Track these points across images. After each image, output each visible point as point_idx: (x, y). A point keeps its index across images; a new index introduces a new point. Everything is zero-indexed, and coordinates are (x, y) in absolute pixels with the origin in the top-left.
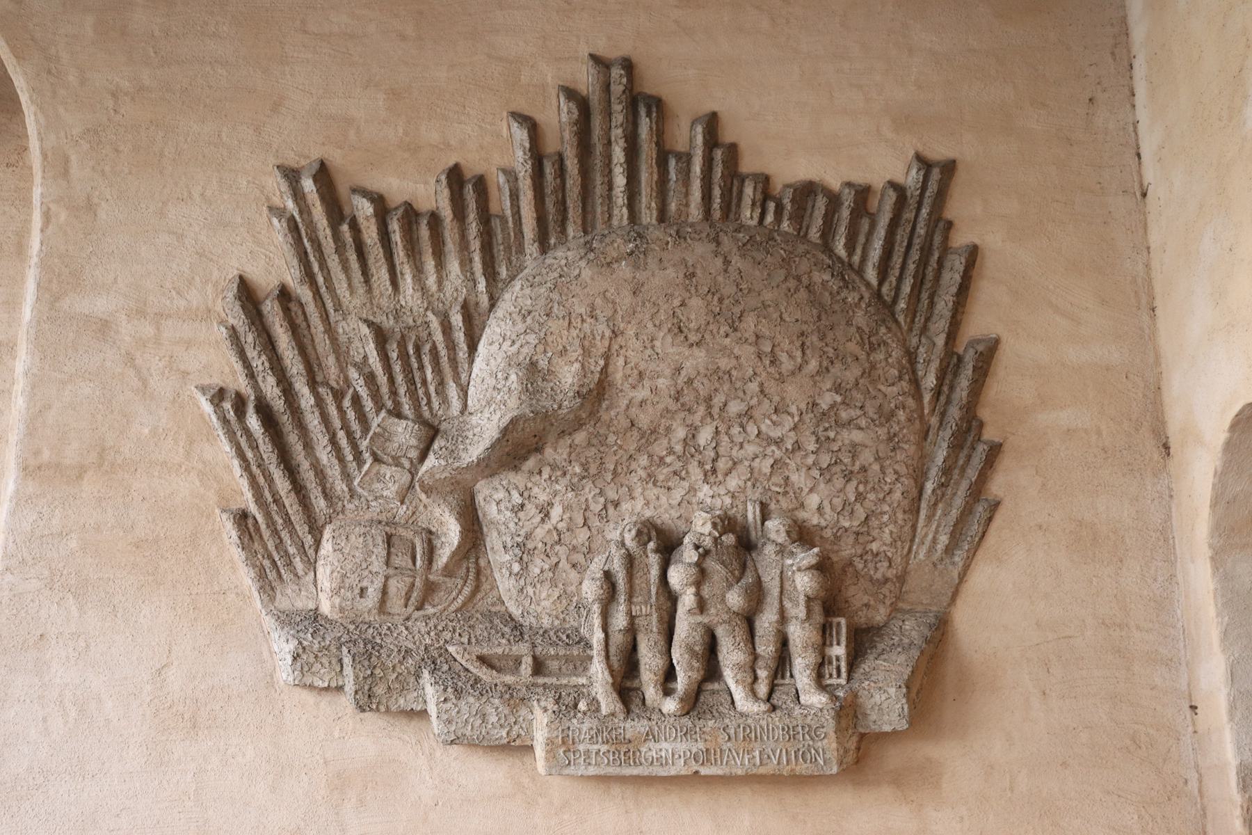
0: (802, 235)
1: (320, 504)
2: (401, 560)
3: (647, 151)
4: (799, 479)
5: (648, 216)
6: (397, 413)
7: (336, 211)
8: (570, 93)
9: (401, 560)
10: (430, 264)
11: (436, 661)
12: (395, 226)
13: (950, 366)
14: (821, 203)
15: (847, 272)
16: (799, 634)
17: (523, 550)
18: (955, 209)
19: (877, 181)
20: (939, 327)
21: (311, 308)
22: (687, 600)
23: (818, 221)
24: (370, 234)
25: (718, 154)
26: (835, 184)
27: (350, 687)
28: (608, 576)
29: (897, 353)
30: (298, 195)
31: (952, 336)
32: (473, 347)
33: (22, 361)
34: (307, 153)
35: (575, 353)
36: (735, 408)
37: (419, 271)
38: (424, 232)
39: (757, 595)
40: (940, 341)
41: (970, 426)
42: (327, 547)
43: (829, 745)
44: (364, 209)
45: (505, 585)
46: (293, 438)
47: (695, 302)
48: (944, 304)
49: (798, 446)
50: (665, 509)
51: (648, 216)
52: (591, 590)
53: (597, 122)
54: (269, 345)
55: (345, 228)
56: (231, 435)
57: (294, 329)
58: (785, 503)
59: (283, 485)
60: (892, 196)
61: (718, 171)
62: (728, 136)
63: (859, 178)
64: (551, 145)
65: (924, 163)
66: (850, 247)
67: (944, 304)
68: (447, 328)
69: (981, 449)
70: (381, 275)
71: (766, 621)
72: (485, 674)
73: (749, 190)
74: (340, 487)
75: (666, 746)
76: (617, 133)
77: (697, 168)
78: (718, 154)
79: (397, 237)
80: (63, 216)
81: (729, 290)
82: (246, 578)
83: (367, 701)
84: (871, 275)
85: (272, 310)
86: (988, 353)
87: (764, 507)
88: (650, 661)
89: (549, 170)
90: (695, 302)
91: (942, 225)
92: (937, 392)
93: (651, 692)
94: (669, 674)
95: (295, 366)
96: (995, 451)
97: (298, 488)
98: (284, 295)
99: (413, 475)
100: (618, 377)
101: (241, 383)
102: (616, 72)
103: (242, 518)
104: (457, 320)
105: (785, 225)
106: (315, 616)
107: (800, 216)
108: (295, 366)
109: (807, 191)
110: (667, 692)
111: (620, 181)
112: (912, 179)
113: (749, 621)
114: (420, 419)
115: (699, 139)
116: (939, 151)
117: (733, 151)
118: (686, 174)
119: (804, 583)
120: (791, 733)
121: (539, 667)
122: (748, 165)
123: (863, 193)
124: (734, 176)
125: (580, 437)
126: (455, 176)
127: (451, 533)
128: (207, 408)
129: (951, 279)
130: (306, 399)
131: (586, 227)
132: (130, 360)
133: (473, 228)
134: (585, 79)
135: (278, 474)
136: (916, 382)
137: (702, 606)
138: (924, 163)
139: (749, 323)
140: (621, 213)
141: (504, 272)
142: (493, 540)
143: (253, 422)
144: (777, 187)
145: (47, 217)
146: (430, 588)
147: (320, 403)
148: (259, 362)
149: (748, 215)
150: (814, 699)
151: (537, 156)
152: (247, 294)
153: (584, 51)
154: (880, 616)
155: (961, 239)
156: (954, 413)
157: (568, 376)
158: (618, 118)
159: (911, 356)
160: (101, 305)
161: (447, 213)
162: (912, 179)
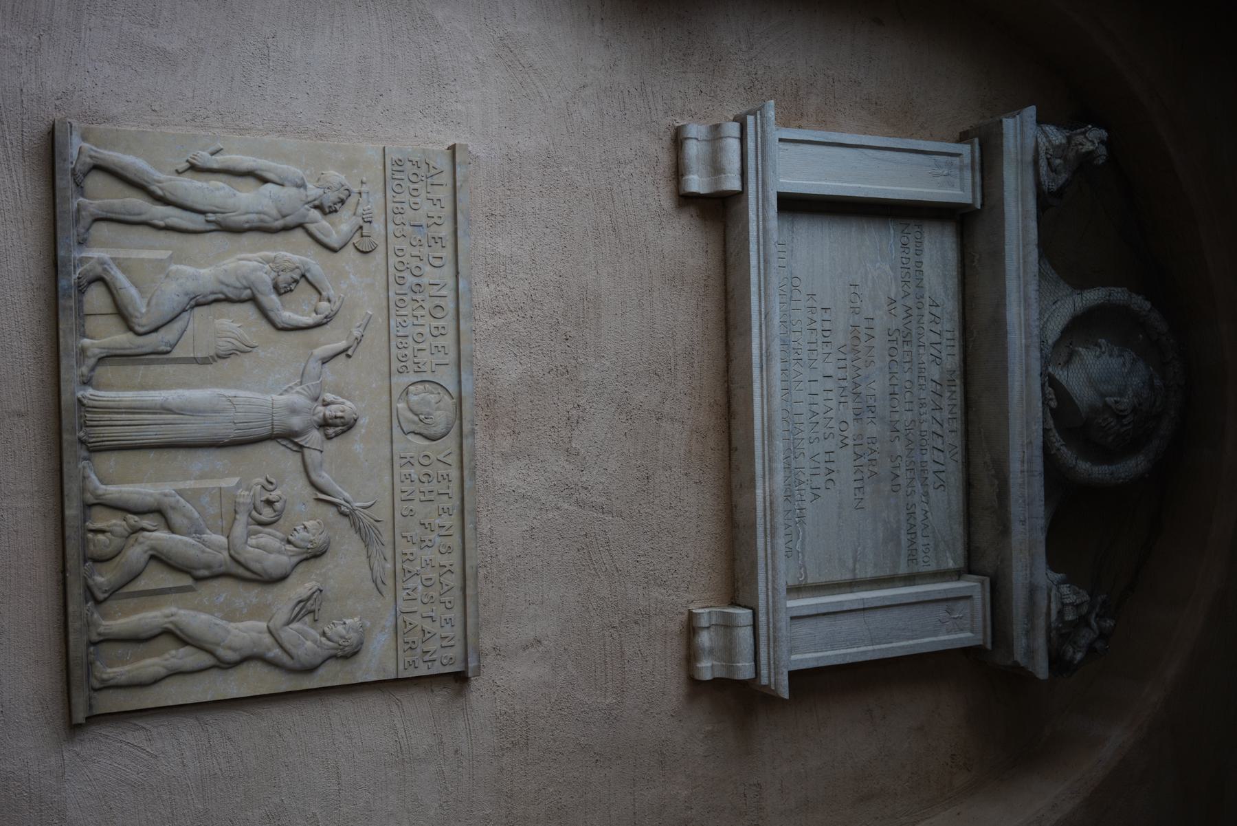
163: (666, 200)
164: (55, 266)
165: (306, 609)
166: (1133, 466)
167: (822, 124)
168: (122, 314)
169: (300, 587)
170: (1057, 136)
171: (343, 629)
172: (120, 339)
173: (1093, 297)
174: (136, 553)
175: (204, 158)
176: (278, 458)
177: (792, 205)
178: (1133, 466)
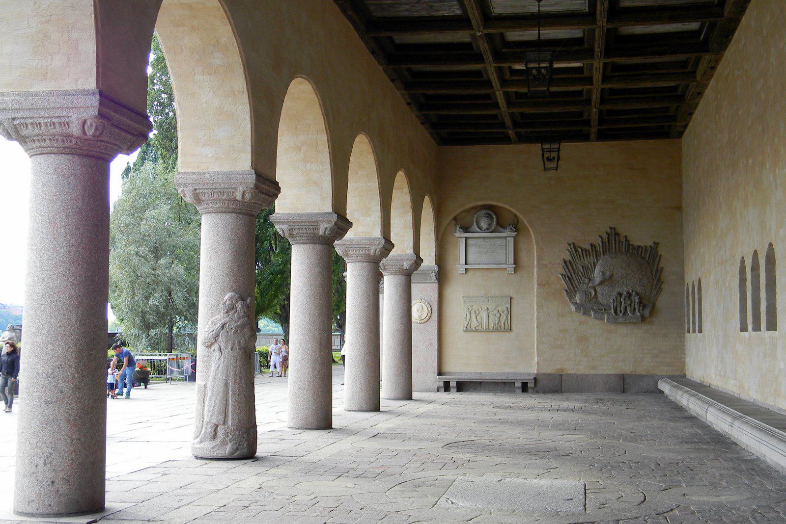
0: (638, 254)
1: (576, 289)
2: (587, 296)
3: (617, 241)
4: (637, 287)
5: (617, 250)
6: (585, 278)
7: (576, 250)
8: (608, 234)
9: (587, 296)
10: (589, 257)
11: (593, 309)
12: (584, 252)
13: (657, 272)
14: (640, 249)
15: (644, 258)
16: (636, 306)
17: (602, 295)
18: (659, 249)
19: (648, 245)
20: (656, 266)
21: (574, 264)
22: (623, 303)
23: (640, 252)
24: (581, 253)
25: (627, 242)
26: (643, 246)
27: (582, 311)
28: (614, 299)
29: (650, 270)
30: (571, 248)
31: (657, 267)
32: (595, 268)
33: (535, 270)
34: (571, 241)
35: (609, 270)
36: (629, 278)
37: (587, 258)
38: (588, 252)
39: (631, 302)
40: (656, 268)
41: (659, 279)
42: (577, 295)
43: (640, 319)
44: (580, 250)
45: (600, 299)
46: (572, 281)
47: (624, 264)
48: (656, 263)
49: (637, 283)
50: (620, 290)
51: (617, 250)
52: (611, 301)
53: (610, 237)
54: (568, 267)
55: (577, 253)
56: (564, 280)
57: (571, 266)
58: (635, 290)
59: (571, 287)
60: (650, 249)
61: (627, 245)
62: (628, 239)
63: (646, 244)
64: (604, 240)
65: (655, 243)
66: (644, 255)
67: (656, 263)
68: (591, 266)
69: (660, 282)
70: (582, 259)
71: (633, 305)
72: (598, 311)
73: (631, 247)
74: (578, 287)
75: (620, 320)
76: (613, 239)
77: (624, 244)
78: (627, 242)
79: (584, 254)
80: (539, 250)
81: (629, 262)
82: (568, 299)
83: (584, 314)
84: (647, 259)
85: (568, 263)
86: (662, 268)
87: (632, 290)
88: (619, 309)
89: (604, 244)
90: (624, 264)
91: (657, 252)
92: (655, 275)
93: (619, 313)
94: (621, 311)
95: (572, 272)
96: (662, 282)
97: (573, 287)
98: (570, 262)
99: (588, 285)
100: (614, 273)
101: (565, 273)
102: (613, 230)
103: (566, 291)
104: (593, 265)
105: (636, 252)
106: (577, 303)
107: (638, 251)
108: (572, 272)
109: (639, 247)
110: (621, 313)
111: (614, 246)
112: (653, 245)
113: (630, 305)
114: (588, 278)
115: (624, 240)
116: (657, 241)
117: (629, 241)
118: (622, 245)
119: (637, 301)
120: (635, 318)
121: (605, 310)
122: (631, 243)
123: (646, 247)
124: (629, 245)
125: (609, 281)
126: (592, 245)
127: (593, 293)
128: (560, 276)
129: (658, 259)
130: (574, 276)
131: (609, 251)
132: (550, 270)
133: (594, 252)
134: (609, 230)
135: (571, 285)
136: (652, 274)
137: (625, 303)
138: (655, 243)
139: (631, 267)
140: (614, 251)
141: (598, 258)
142: (598, 294)
143: (567, 279)
144: (635, 246)
145: (537, 250)
146: (591, 300)
147: (575, 276)
148: (567, 271)
149: (631, 251)
150: (638, 314)
151: (602, 242)
152: (565, 262)
153: (608, 226)
154: (647, 303)
155: (659, 254)
156: (657, 277)
157: (608, 274)
158: (613, 237)
159: (652, 270)
160: (545, 262)
161: (591, 250)
162: (653, 245)
163: (466, 275)
164: (474, 331)
165: (503, 312)
166: (494, 217)
167: (458, 256)
168: (478, 326)
169: (501, 313)
170: (457, 231)
171: (505, 309)
172: (480, 326)
173: (475, 223)
174: (497, 326)
175: (465, 319)
176: (489, 314)
177: (466, 264)
178: (494, 217)
